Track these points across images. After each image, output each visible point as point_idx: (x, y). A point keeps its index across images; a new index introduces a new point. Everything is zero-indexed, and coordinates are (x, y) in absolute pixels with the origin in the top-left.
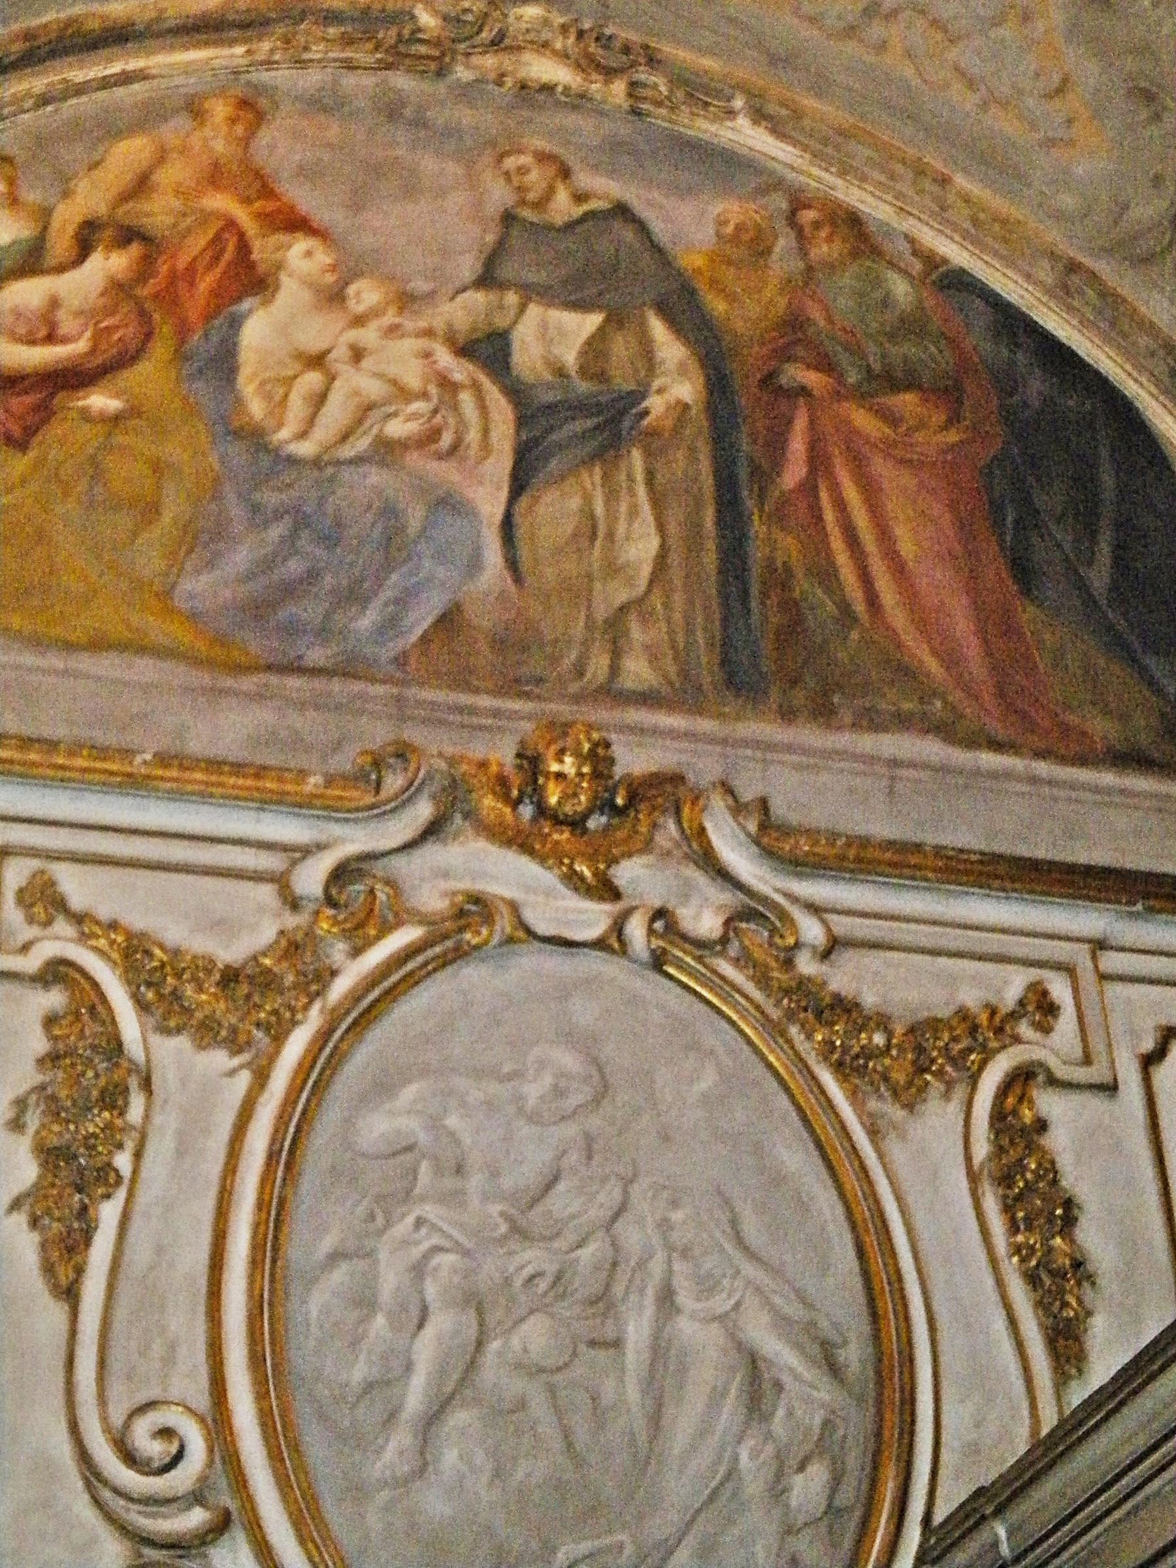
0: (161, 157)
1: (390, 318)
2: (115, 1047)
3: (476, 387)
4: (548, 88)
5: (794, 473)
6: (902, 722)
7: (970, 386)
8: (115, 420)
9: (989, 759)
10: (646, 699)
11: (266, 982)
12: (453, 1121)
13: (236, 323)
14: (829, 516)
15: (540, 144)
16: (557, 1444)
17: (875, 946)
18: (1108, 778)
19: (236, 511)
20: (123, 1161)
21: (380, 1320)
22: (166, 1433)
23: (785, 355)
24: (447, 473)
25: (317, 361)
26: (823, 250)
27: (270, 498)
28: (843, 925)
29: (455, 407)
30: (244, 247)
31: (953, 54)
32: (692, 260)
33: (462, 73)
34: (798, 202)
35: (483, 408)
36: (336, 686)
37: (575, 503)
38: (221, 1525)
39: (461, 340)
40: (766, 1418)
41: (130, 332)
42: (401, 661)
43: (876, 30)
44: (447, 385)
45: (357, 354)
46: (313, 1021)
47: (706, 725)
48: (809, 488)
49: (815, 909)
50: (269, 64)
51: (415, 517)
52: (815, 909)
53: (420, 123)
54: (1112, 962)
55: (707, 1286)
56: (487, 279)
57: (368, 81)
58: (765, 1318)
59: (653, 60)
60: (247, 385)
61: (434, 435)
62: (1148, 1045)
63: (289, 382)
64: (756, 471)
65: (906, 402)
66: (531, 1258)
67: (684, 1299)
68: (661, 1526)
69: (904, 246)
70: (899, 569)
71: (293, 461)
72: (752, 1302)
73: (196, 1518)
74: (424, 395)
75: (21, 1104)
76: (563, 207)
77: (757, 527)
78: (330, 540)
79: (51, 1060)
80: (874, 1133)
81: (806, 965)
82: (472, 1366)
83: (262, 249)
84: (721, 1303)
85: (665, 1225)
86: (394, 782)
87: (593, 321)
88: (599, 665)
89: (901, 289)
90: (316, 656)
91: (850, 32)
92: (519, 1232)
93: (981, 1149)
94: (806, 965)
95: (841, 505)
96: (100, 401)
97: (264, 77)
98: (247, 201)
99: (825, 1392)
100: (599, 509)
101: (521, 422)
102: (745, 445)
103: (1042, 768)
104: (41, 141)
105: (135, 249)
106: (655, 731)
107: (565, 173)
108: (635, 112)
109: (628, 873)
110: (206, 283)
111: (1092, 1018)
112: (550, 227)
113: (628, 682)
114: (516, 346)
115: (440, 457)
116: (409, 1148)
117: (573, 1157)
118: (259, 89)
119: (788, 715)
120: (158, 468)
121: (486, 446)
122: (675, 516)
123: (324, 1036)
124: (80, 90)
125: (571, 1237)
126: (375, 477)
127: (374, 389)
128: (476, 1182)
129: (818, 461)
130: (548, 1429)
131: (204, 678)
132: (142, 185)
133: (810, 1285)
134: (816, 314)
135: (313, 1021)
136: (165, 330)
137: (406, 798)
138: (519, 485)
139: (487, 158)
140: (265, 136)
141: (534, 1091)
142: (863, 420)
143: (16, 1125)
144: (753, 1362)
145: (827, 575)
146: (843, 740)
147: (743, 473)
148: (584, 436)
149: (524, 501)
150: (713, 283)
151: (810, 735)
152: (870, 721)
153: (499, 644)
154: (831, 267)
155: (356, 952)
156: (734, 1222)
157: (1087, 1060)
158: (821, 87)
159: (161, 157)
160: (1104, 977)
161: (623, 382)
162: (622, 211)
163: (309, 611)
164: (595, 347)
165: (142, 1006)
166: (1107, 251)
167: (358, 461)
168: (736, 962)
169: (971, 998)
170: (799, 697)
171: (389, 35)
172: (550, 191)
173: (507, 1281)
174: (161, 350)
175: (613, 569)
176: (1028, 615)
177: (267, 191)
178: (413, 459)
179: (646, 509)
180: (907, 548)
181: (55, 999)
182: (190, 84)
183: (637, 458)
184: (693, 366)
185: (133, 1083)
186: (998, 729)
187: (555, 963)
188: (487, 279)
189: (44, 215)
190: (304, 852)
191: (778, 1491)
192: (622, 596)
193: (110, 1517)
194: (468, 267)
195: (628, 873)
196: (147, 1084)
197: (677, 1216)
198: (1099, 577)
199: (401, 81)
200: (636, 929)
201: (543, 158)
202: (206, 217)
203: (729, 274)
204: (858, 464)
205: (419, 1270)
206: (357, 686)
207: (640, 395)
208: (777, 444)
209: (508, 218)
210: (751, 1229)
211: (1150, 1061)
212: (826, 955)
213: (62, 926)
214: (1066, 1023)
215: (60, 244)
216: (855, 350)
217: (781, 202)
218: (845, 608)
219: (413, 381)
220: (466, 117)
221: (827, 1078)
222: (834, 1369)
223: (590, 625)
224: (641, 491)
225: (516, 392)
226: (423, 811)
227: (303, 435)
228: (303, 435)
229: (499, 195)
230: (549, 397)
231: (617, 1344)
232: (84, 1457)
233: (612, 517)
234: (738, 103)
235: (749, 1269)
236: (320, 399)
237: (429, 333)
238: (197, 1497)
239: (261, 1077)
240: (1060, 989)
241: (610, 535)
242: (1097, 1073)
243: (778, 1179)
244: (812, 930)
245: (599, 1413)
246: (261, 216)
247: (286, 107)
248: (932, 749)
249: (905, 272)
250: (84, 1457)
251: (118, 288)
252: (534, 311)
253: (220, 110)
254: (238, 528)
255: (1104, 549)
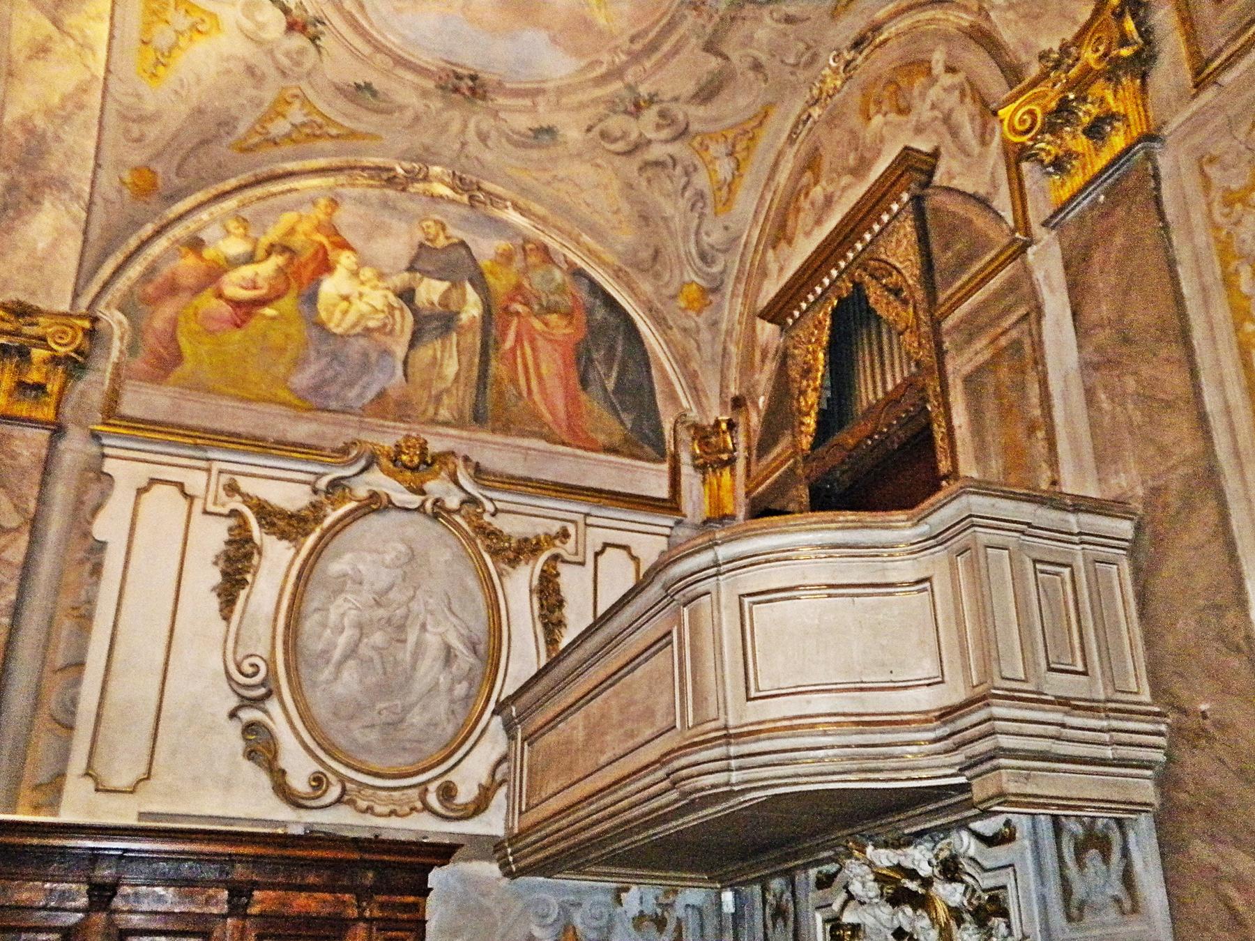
0: (300, 220)
1: (375, 282)
2: (250, 539)
3: (401, 309)
4: (441, 197)
5: (509, 343)
6: (533, 434)
7: (577, 314)
8: (273, 318)
9: (561, 448)
10: (446, 424)
11: (304, 520)
12: (361, 567)
13: (318, 283)
14: (519, 360)
15: (437, 217)
16: (381, 672)
17: (509, 512)
18: (602, 456)
19: (313, 354)
20: (249, 577)
21: (329, 631)
22: (252, 665)
23: (512, 299)
24: (388, 340)
25: (346, 298)
26: (533, 259)
27: (324, 348)
28: (499, 505)
29: (393, 316)
30: (326, 253)
31: (583, 195)
32: (484, 263)
33: (412, 190)
34: (527, 240)
35: (403, 317)
36: (341, 417)
37: (430, 352)
38: (268, 695)
39: (398, 291)
40: (450, 666)
41: (282, 287)
42: (363, 409)
43: (556, 185)
44: (391, 307)
45: (361, 295)
46: (318, 531)
47: (465, 434)
48: (513, 350)
49: (491, 500)
50: (342, 185)
51: (374, 356)
52: (491, 500)
53: (395, 208)
54: (590, 520)
55: (438, 624)
56: (411, 269)
57: (377, 192)
58: (455, 634)
59: (479, 189)
60: (321, 306)
61: (385, 325)
62: (598, 549)
63: (335, 305)
64: (496, 342)
65: (553, 318)
66: (381, 612)
67: (429, 627)
68: (413, 698)
69: (562, 258)
70: (540, 378)
71: (334, 334)
72: (452, 629)
73: (262, 691)
74: (383, 311)
75: (217, 557)
76: (441, 242)
77: (493, 363)
78: (342, 364)
79: (229, 543)
80: (500, 576)
81: (487, 518)
82: (357, 646)
83: (332, 255)
84: (441, 629)
85: (426, 603)
86: (354, 453)
87: (446, 284)
88: (431, 411)
89: (558, 275)
90: (333, 405)
91: (549, 183)
92: (378, 604)
93: (535, 582)
94: (487, 518)
95: (523, 355)
96: (269, 311)
97: (340, 190)
98: (328, 237)
99: (472, 659)
100: (439, 355)
101: (416, 322)
102: (494, 331)
103: (579, 452)
104: (258, 214)
105: (287, 255)
106: (447, 436)
107: (444, 229)
108: (472, 206)
109: (430, 486)
110: (311, 267)
111: (581, 540)
112: (435, 249)
113: (440, 418)
114: (417, 293)
115: (385, 334)
116: (344, 576)
117: (399, 581)
118: (337, 194)
119: (494, 431)
120: (287, 336)
121: (402, 331)
122: (465, 359)
123: (321, 538)
124: (274, 195)
125: (395, 606)
126: (363, 342)
127: (365, 308)
128: (366, 587)
129: (519, 339)
130: (379, 667)
131: (292, 413)
132: (292, 231)
133: (472, 624)
134: (526, 284)
135: (318, 531)
136: (294, 284)
137: (357, 459)
138: (412, 345)
139: (416, 222)
140: (337, 213)
141: (388, 558)
142: (538, 325)
143: (216, 563)
144: (448, 649)
145: (514, 381)
146: (510, 440)
147: (491, 342)
148: (435, 329)
149: (412, 352)
150: (491, 273)
151: (499, 438)
152: (522, 434)
153: (398, 404)
154: (535, 266)
155: (334, 510)
156: (450, 603)
157: (576, 554)
158: (538, 200)
159: (300, 220)
160: (586, 525)
161: (454, 308)
162: (463, 244)
163: (334, 389)
164: (446, 295)
165: (261, 526)
166: (631, 265)
167: (358, 335)
168: (463, 517)
169: (540, 531)
170: (498, 425)
171: (385, 176)
172: (437, 235)
173: (371, 620)
174: (293, 293)
175: (441, 377)
176: (583, 397)
177: (337, 234)
178: (376, 335)
179: (455, 353)
180: (544, 370)
181: (232, 522)
182: (313, 193)
183: (454, 337)
184: (479, 303)
185: (255, 551)
186: (565, 438)
187: (404, 516)
188: (411, 269)
189: (256, 241)
190: (319, 476)
191: (451, 690)
192: (443, 386)
193: (235, 691)
194: (404, 263)
195: (430, 486)
196: (260, 553)
197: (431, 601)
198: (610, 385)
199: (391, 193)
200: (428, 505)
201: (436, 222)
202: (313, 241)
203: (498, 269)
204: (532, 341)
205: (343, 615)
206: (348, 416)
207: (458, 313)
208: (504, 334)
209: (421, 245)
210: (456, 607)
211: (597, 555)
212: (493, 515)
213: (238, 498)
214: (571, 541)
215: (261, 253)
216: (538, 298)
217: (520, 241)
218: (520, 394)
219: (379, 306)
220: (411, 206)
221: (487, 557)
222: (475, 652)
223: (430, 396)
224: (454, 349)
225: (415, 312)
226: (362, 463)
227: (338, 326)
228: (338, 326)
229: (419, 236)
230: (427, 313)
231: (404, 641)
232: (227, 672)
233: (442, 356)
234: (509, 204)
235: (453, 619)
236: (345, 313)
237: (388, 288)
238: (263, 684)
239: (298, 553)
240: (571, 529)
241: (441, 365)
242: (579, 559)
243: (465, 589)
244: (489, 506)
245: (396, 663)
246: (333, 243)
247: (348, 201)
248: (541, 444)
249: (560, 268)
250: (227, 672)
251: (280, 270)
252: (426, 280)
253: (323, 202)
254: (312, 358)
255: (614, 374)
